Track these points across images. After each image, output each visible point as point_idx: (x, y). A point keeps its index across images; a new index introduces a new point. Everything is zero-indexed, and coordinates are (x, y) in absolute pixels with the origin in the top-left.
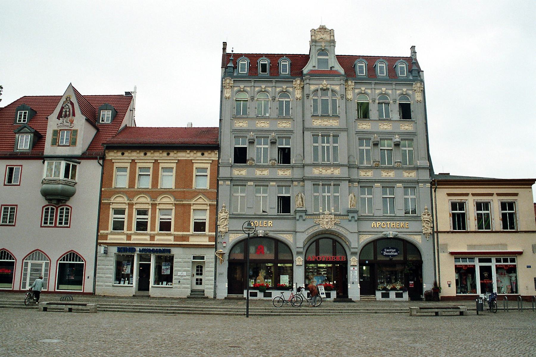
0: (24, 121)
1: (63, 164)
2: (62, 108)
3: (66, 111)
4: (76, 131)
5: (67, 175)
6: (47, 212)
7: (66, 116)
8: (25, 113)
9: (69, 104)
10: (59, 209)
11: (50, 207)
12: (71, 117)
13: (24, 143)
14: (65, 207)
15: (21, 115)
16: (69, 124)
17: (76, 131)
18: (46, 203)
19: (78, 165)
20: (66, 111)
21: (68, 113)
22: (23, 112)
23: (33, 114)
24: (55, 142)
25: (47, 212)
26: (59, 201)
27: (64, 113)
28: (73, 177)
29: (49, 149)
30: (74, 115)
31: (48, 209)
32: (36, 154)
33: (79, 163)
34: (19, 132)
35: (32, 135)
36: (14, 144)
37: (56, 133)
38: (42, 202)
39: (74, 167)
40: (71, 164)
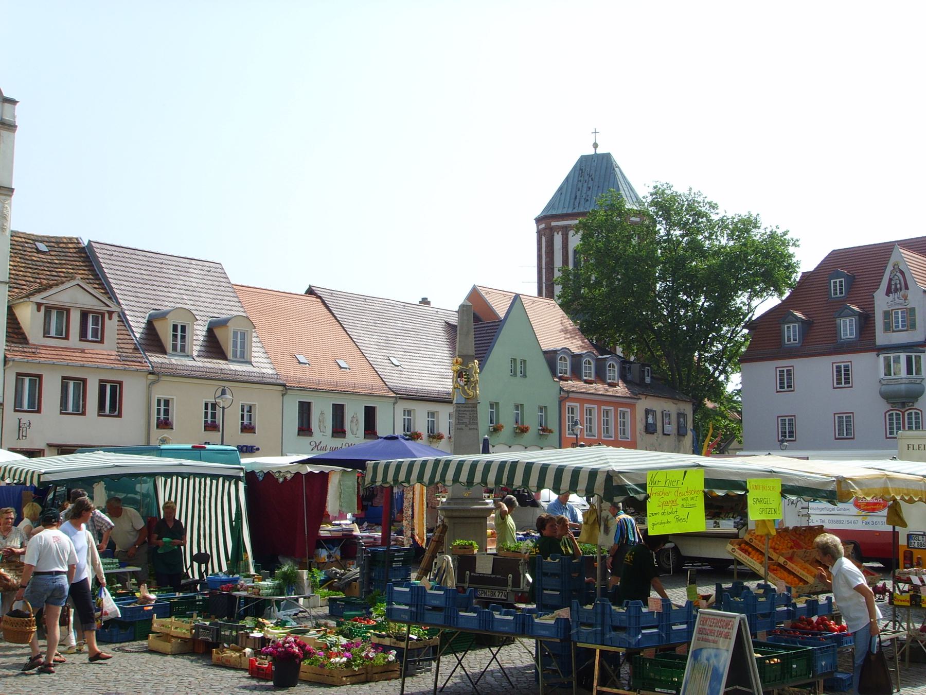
0: (841, 293)
1: (903, 356)
2: (890, 280)
3: (896, 284)
4: (912, 310)
5: (909, 371)
6: (891, 419)
7: (896, 290)
8: (841, 282)
9: (898, 274)
10: (906, 413)
11: (894, 412)
12: (903, 291)
13: (847, 329)
14: (913, 411)
15: (835, 286)
16: (902, 301)
17: (912, 310)
18: (889, 407)
19: (922, 355)
20: (896, 284)
21: (898, 286)
22: (838, 280)
23: (852, 281)
24: (888, 328)
25: (891, 419)
26: (903, 404)
27: (893, 287)
28: (918, 371)
29: (882, 338)
30: (907, 288)
31: (891, 415)
32: (865, 341)
33: (924, 352)
34: (840, 316)
35: (857, 317)
36: (835, 331)
37: (887, 314)
38: (885, 406)
39: (918, 359)
40: (913, 355)
